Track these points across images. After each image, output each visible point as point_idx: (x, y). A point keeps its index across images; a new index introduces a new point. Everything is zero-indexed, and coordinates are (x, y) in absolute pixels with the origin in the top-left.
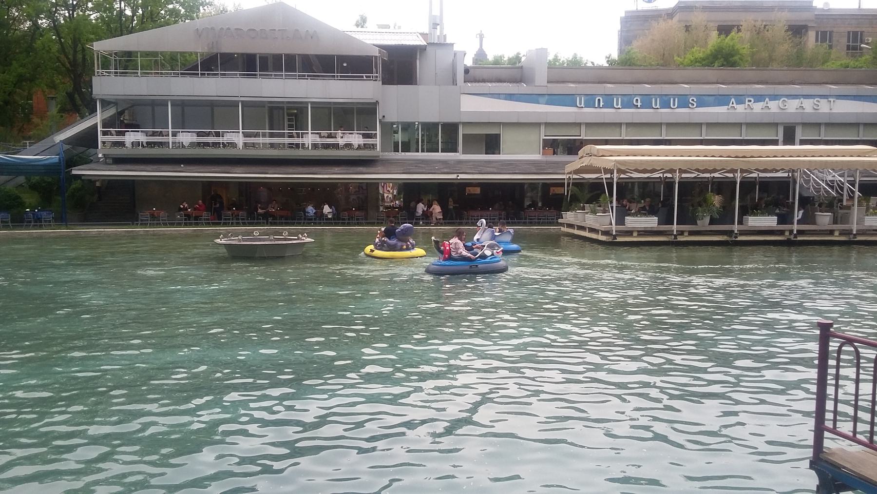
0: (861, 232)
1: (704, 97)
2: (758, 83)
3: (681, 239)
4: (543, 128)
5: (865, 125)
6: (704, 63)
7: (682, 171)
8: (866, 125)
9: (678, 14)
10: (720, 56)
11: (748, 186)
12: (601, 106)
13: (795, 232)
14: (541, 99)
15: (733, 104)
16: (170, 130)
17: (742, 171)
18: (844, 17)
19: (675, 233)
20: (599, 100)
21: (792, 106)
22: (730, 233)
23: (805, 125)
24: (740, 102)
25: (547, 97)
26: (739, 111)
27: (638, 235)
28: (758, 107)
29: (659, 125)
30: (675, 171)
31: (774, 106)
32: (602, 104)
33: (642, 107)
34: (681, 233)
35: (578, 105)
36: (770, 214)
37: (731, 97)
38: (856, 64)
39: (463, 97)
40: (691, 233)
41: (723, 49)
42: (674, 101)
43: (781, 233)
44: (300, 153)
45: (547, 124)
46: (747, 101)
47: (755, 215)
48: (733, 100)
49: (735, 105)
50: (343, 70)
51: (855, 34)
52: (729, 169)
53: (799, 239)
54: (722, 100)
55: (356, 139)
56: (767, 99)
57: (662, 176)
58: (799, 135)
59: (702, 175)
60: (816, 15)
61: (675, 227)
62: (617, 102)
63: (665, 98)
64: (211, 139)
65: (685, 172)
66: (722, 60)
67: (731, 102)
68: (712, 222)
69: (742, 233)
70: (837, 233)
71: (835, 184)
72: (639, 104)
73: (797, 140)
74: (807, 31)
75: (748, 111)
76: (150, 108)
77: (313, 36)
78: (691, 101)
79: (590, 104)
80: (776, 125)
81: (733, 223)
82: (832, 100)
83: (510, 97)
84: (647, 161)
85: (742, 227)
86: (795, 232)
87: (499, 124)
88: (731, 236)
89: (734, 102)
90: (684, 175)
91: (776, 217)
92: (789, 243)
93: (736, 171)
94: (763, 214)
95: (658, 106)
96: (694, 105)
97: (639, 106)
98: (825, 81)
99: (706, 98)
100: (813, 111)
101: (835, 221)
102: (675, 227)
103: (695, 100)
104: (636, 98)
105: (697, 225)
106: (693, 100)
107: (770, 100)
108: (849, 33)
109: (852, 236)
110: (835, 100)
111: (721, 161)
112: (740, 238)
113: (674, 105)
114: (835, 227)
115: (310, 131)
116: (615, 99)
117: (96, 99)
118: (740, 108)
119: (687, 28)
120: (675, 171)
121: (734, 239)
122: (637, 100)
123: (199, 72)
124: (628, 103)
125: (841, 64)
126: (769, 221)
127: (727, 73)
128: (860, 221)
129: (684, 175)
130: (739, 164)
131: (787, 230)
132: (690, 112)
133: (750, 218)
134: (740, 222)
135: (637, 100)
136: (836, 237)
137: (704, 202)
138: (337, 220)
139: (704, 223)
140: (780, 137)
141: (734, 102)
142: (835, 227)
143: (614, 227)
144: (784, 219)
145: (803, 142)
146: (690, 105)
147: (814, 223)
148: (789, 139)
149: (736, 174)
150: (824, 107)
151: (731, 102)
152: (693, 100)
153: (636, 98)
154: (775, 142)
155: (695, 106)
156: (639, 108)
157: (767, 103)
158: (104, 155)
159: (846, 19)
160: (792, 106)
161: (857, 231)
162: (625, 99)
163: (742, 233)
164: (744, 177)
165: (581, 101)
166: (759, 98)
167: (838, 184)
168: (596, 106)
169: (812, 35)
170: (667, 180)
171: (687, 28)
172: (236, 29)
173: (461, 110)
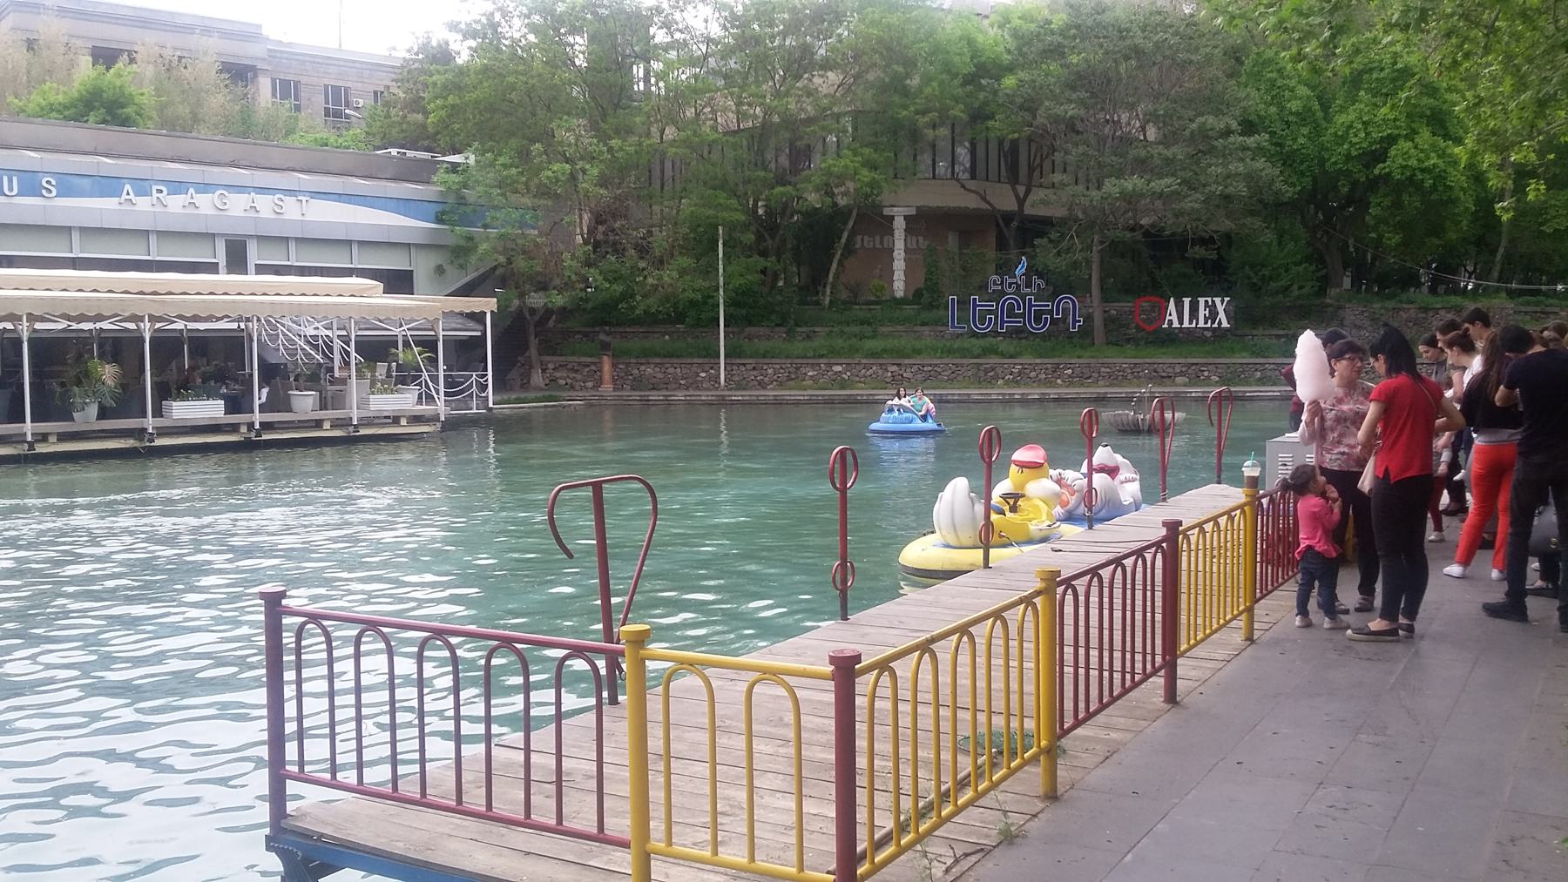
0: (368, 422)
2: (172, 160)
3: (41, 448)
5: (362, 243)
6: (66, 113)
7: (32, 318)
8: (363, 244)
9: (11, 14)
10: (97, 104)
11: (167, 346)
13: (257, 427)
15: (128, 194)
17: (153, 319)
18: (317, 60)
19: (29, 438)
21: (238, 205)
22: (140, 433)
23: (262, 239)
24: (143, 192)
26: (142, 209)
28: (176, 203)
30: (19, 318)
31: (206, 203)
34: (44, 438)
37: (125, 181)
38: (340, 141)
40: (64, 437)
41: (103, 91)
42: (10, 181)
43: (234, 428)
46: (155, 188)
48: (128, 187)
49: (132, 196)
51: (336, 89)
52: (127, 314)
53: (265, 437)
54: (108, 185)
56: (191, 190)
58: (254, 256)
59: (75, 326)
60: (269, 50)
61: (28, 427)
65: (42, 319)
66: (103, 111)
67: (125, 192)
68: (103, 414)
69: (163, 432)
70: (327, 425)
71: (321, 341)
73: (251, 267)
74: (255, 76)
75: (159, 209)
80: (211, 237)
81: (144, 415)
82: (304, 199)
85: (161, 422)
86: (257, 427)
88: (141, 440)
89: (131, 192)
90: (38, 326)
91: (223, 402)
92: (248, 446)
93: (141, 319)
94: (198, 397)
96: (50, 191)
98: (290, 165)
99: (77, 180)
100: (274, 216)
101: (323, 406)
102: (28, 427)
103: (54, 183)
105: (74, 420)
106: (48, 182)
107: (196, 193)
108: (326, 87)
109: (351, 429)
110: (308, 198)
111: (110, 300)
112: (159, 442)
113: (11, 189)
118: (143, 203)
119: (31, 45)
120: (19, 318)
121: (148, 444)
125: (316, 140)
126: (211, 409)
127: (113, 136)
128: (363, 404)
129: (38, 326)
130: (146, 306)
131: (244, 424)
132: (44, 206)
133: (174, 404)
134: (158, 413)
136: (327, 432)
137: (84, 377)
139: (87, 416)
140: (221, 259)
141: (131, 192)
144: (236, 404)
145: (261, 269)
146: (44, 192)
147: (290, 411)
148: (237, 261)
149: (142, 324)
150: (293, 210)
151: (125, 192)
152: (48, 182)
154: (212, 268)
157: (192, 198)
159: (319, 63)
160: (238, 205)
161: (360, 419)
163: (163, 432)
166: (177, 187)
167: (324, 342)
169: (264, 85)
171: (31, 45)
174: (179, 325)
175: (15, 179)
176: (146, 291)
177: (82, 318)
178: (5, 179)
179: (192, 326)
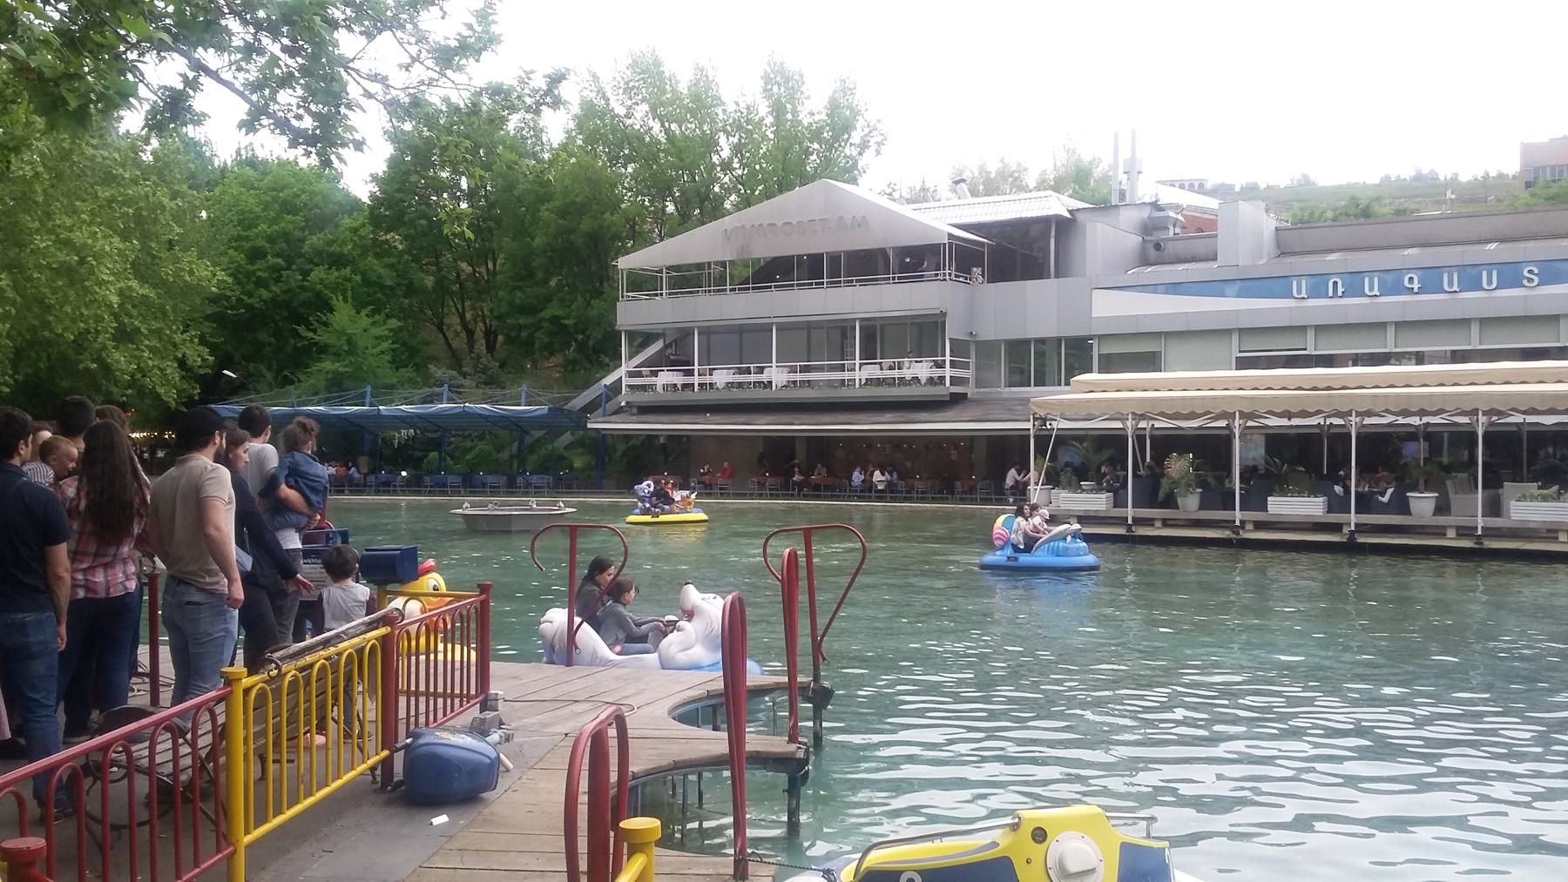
1: (1556, 264)
4: (1235, 337)
12: (1340, 294)
14: (1229, 289)
17: (1243, 415)
20: (1335, 283)
25: (1239, 284)
27: (1458, 535)
29: (1464, 323)
32: (1340, 290)
33: (1421, 291)
34: (1148, 522)
35: (1446, 288)
36: (1314, 493)
39: (1095, 292)
40: (1166, 523)
43: (1336, 528)
44: (844, 394)
45: (1243, 332)
47: (1283, 493)
50: (904, 268)
53: (1361, 539)
55: (921, 369)
57: (1322, 423)
59: (1401, 421)
62: (1371, 285)
63: (1474, 271)
64: (753, 378)
65: (1369, 414)
69: (1259, 526)
70: (1451, 533)
72: (1416, 286)
76: (804, 334)
77: (861, 223)
78: (1526, 274)
79: (1317, 291)
83: (1174, 288)
84: (1432, 395)
87: (1157, 335)
92: (1351, 548)
95: (1455, 288)
97: (1416, 290)
103: (1536, 271)
104: (1410, 275)
105: (1411, 514)
106: (1530, 271)
113: (1490, 282)
114: (1441, 520)
116: (1367, 280)
117: (620, 332)
122: (1411, 279)
124: (1391, 283)
126: (1310, 507)
134: (1255, 500)
135: (1411, 279)
136: (1451, 540)
138: (890, 492)
142: (1441, 520)
153: (1410, 275)
155: (1535, 284)
156: (1417, 293)
158: (627, 403)
162: (1390, 278)
164: (1492, 424)
165: (1300, 287)
168: (1331, 294)
170: (1332, 431)
172: (770, 225)
174: (1517, 418)
175: (1495, 273)
176: (1319, 386)
177: (1405, 413)
178: (1485, 274)
179: (1531, 419)
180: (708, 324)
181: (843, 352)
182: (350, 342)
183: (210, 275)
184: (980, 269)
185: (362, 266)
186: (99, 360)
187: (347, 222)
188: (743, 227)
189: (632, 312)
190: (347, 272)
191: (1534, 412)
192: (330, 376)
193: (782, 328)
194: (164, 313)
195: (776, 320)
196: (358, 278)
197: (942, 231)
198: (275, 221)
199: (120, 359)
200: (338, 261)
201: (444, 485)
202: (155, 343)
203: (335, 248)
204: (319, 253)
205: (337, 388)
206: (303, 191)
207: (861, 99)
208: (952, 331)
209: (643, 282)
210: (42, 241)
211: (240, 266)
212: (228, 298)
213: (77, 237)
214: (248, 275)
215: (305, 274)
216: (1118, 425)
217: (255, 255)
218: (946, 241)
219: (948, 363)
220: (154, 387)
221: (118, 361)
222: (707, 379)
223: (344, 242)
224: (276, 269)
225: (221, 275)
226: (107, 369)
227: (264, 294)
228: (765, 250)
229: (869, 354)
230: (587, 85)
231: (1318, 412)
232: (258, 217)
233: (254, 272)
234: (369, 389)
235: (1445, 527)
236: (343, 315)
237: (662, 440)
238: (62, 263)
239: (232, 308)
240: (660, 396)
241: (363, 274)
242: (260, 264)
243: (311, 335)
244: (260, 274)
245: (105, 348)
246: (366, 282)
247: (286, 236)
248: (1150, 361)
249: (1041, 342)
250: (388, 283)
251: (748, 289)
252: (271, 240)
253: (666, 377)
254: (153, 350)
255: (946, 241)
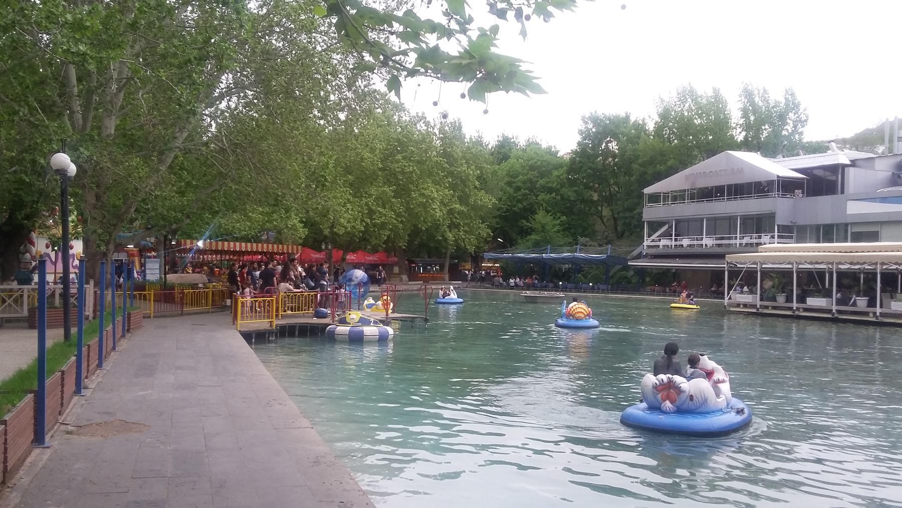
16: (738, 235)
34: (767, 307)
69: (806, 310)
77: (741, 171)
81: (875, 307)
92: (835, 320)
115: (704, 236)
123: (726, 198)
134: (802, 299)
143: (759, 303)
173: (848, 213)
176: (848, 251)
180: (687, 217)
181: (732, 230)
182: (543, 226)
183: (487, 200)
184: (800, 191)
185: (561, 192)
186: (443, 236)
187: (556, 173)
188: (693, 174)
189: (650, 213)
190: (553, 195)
191: (817, 263)
192: (533, 241)
193: (708, 219)
194: (471, 217)
195: (705, 216)
196: (559, 197)
197: (774, 174)
198: (528, 174)
199: (450, 236)
200: (550, 190)
201: (566, 288)
202: (466, 228)
203: (550, 185)
204: (543, 187)
205: (537, 246)
206: (539, 160)
207: (799, 98)
208: (780, 220)
209: (655, 198)
210: (415, 194)
211: (511, 194)
212: (502, 209)
213: (427, 192)
214: (514, 198)
215: (537, 196)
216: (790, 266)
217: (518, 189)
218: (776, 179)
219: (673, 240)
220: (465, 246)
221: (449, 236)
222: (678, 243)
223: (553, 182)
224: (524, 195)
225: (494, 200)
226: (446, 240)
227: (520, 205)
228: (702, 184)
229: (745, 231)
230: (658, 104)
231: (822, 263)
232: (520, 173)
233: (517, 196)
234: (549, 246)
235: (869, 312)
236: (541, 217)
237: (674, 271)
238: (421, 202)
239: (504, 213)
240: (660, 251)
241: (561, 195)
242: (519, 193)
243: (528, 224)
244: (518, 197)
245: (445, 231)
246: (563, 198)
247: (531, 181)
248: (874, 236)
249: (825, 226)
250: (572, 199)
251: (694, 202)
252: (524, 183)
253: (664, 242)
254: (465, 231)
255: (776, 179)
